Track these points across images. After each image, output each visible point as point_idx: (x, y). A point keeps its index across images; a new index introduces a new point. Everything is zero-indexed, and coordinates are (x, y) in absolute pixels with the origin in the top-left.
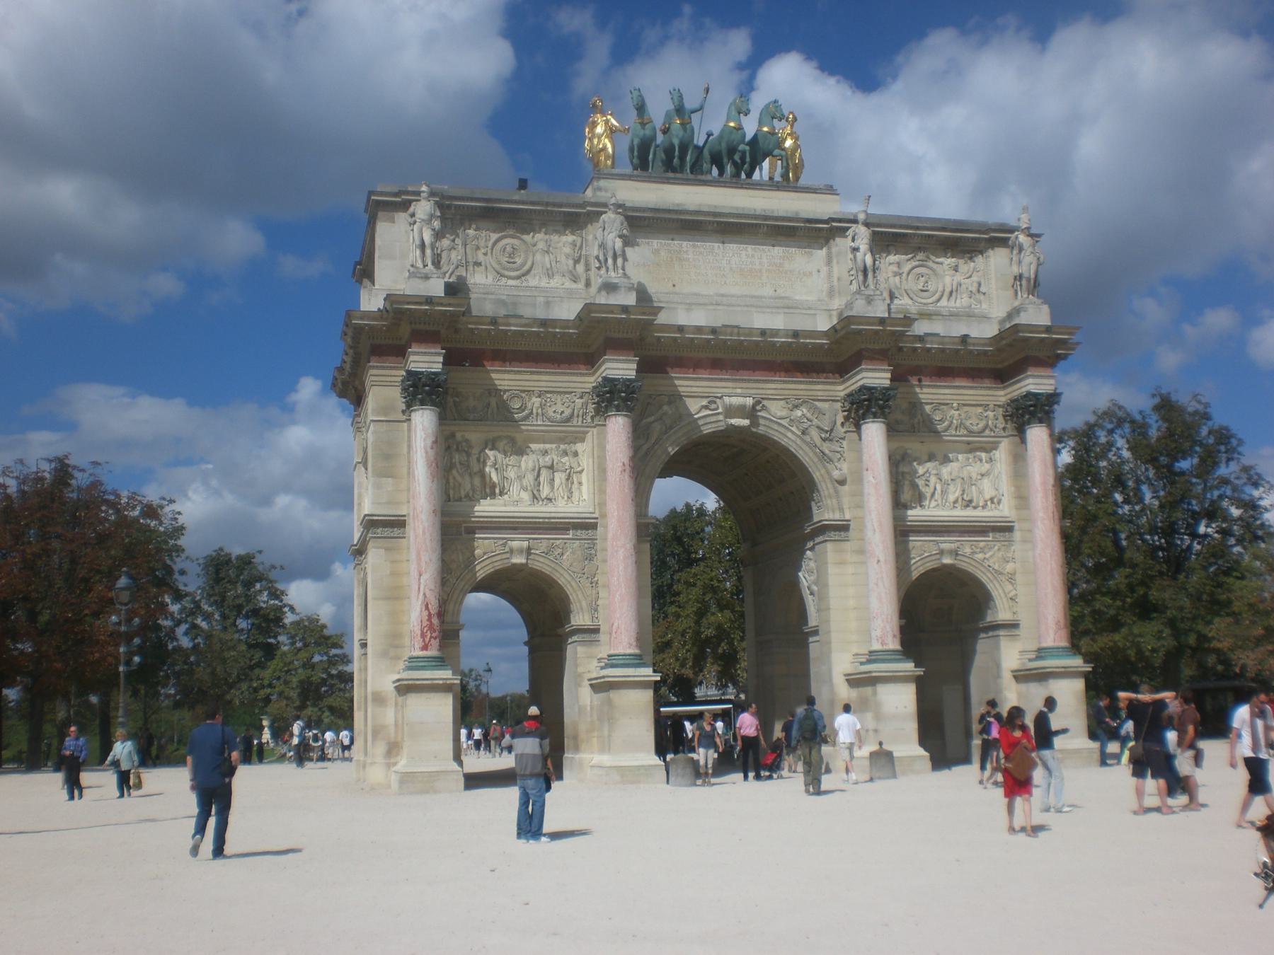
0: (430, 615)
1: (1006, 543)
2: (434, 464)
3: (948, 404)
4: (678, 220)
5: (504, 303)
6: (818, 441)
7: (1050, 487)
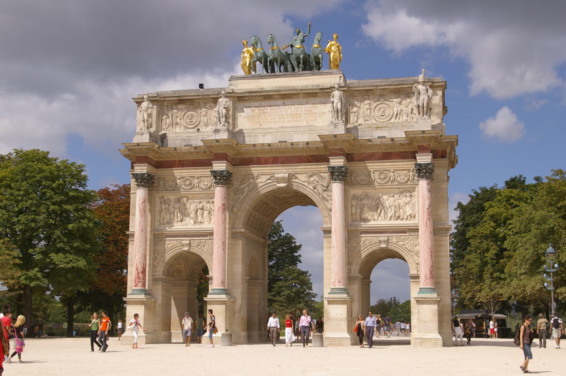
0: (138, 273)
1: (416, 237)
2: (142, 211)
3: (389, 170)
4: (261, 96)
5: (184, 140)
6: (321, 191)
7: (426, 209)
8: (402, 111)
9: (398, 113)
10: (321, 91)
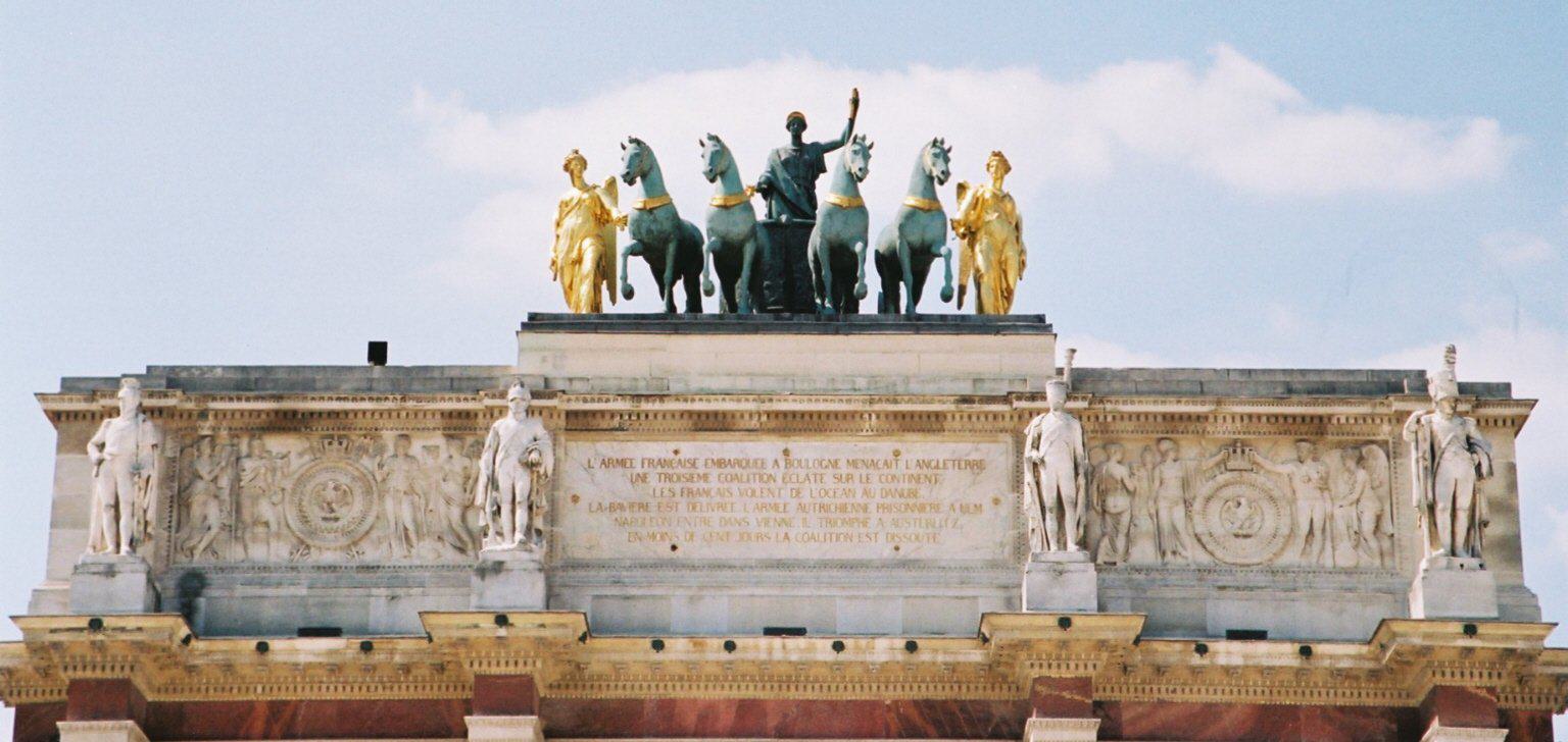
4: (682, 414)
8: (1332, 517)
9: (1318, 526)
10: (964, 406)
